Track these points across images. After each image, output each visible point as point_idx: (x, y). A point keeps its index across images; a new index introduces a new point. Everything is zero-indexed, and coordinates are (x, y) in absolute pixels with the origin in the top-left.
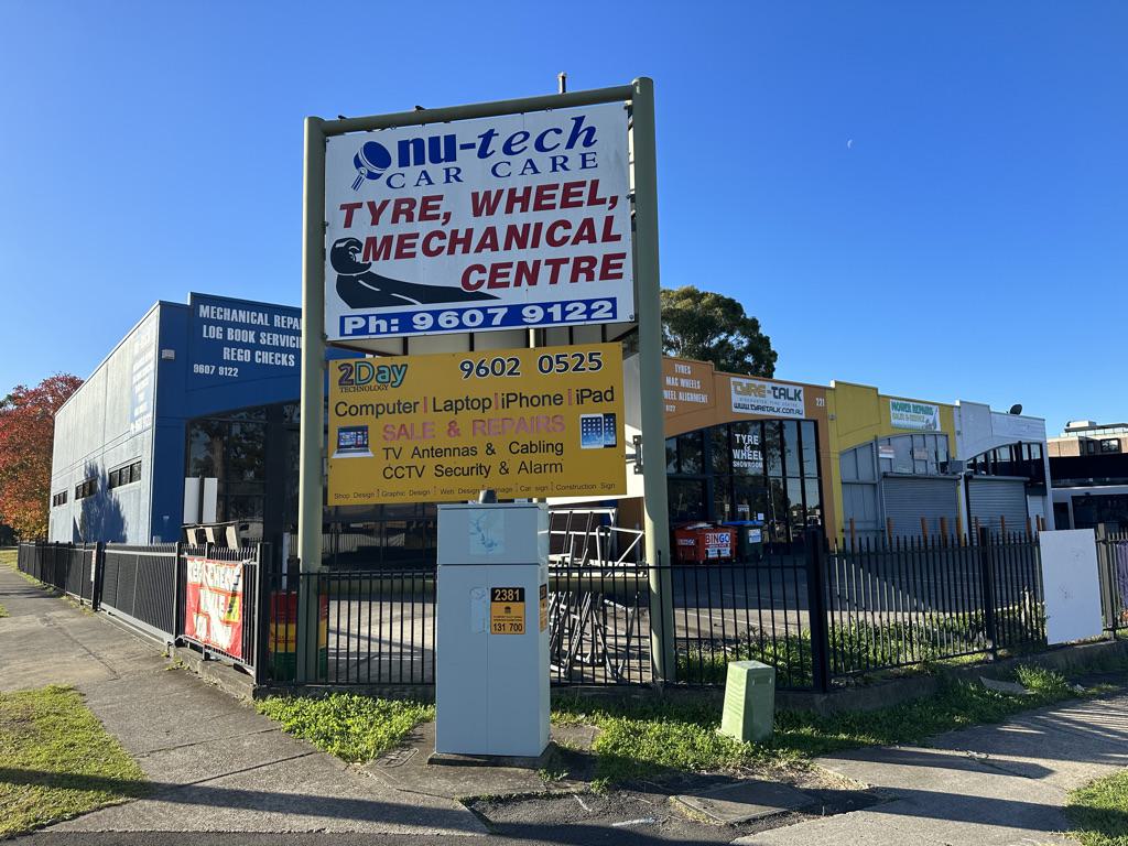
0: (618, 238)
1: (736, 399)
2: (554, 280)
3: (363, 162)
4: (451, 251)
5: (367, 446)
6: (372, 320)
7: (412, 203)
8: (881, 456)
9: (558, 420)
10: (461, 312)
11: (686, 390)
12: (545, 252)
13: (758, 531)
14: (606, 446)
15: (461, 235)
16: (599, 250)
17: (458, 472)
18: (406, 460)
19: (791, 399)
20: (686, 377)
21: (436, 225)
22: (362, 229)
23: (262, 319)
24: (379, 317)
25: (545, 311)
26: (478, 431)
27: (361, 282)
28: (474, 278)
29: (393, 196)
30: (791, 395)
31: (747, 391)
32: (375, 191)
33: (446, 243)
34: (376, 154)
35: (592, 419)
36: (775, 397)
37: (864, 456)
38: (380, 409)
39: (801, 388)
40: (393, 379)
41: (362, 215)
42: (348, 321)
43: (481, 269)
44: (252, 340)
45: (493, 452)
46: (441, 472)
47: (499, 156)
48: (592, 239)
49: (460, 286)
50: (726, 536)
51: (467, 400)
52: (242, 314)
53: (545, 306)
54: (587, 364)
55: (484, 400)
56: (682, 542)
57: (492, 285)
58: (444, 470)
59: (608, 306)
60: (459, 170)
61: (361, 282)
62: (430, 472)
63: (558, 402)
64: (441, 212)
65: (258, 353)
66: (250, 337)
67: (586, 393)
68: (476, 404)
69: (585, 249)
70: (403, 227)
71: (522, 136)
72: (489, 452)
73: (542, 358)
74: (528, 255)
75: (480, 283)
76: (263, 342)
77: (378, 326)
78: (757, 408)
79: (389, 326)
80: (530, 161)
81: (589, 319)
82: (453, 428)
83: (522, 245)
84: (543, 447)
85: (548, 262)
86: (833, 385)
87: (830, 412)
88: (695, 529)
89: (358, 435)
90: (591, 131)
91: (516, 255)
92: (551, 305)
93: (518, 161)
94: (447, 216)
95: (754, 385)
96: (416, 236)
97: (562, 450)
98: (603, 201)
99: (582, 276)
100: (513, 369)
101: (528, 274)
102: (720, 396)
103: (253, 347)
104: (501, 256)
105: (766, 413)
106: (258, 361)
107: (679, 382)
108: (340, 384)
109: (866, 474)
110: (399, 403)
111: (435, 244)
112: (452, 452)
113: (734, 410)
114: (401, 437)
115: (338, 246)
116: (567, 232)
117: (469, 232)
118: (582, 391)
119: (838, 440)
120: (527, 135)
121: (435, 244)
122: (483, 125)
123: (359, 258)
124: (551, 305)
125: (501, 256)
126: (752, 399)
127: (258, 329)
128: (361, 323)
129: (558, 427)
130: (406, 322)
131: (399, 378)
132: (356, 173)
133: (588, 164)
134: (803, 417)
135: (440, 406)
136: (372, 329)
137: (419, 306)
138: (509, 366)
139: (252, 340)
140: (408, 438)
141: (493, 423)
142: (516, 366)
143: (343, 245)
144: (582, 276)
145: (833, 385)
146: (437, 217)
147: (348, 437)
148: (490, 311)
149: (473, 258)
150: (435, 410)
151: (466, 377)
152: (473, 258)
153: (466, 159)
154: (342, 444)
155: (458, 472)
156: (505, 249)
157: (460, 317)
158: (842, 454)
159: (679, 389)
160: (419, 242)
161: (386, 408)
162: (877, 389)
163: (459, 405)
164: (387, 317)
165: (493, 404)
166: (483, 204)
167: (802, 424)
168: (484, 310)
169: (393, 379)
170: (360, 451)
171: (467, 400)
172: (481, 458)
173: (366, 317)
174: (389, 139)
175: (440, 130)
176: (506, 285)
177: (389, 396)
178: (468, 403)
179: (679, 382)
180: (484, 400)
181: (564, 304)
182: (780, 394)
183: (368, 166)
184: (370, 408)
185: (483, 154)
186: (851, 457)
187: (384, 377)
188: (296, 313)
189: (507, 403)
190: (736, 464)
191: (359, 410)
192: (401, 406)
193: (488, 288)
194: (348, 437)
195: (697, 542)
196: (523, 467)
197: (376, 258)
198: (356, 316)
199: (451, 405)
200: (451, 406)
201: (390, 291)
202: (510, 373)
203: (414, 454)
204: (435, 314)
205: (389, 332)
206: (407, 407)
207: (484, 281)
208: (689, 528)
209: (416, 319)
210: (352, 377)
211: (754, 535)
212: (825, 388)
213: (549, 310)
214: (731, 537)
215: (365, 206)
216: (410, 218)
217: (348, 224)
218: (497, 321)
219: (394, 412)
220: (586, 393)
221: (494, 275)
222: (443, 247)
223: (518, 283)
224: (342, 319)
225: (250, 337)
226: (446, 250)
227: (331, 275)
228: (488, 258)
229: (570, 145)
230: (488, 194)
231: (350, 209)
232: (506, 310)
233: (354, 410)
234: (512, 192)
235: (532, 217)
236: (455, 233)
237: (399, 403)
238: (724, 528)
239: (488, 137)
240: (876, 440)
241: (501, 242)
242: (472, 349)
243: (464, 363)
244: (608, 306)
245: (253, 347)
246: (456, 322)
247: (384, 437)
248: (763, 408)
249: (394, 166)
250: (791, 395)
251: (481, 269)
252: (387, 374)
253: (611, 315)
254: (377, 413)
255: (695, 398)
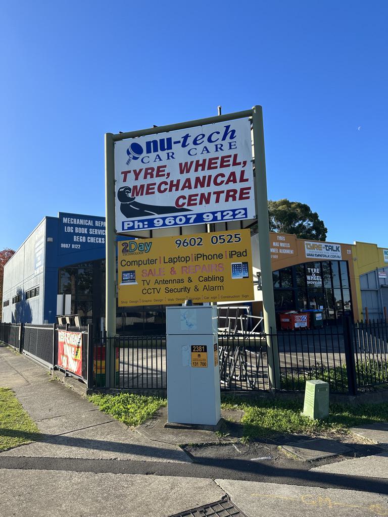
0: (247, 180)
1: (307, 251)
2: (217, 201)
3: (131, 152)
4: (171, 190)
5: (135, 279)
6: (136, 223)
7: (153, 169)
8: (379, 277)
9: (220, 265)
10: (175, 217)
11: (283, 248)
12: (213, 188)
13: (320, 314)
14: (244, 277)
15: (175, 183)
16: (238, 186)
17: (175, 290)
18: (152, 285)
19: (335, 251)
20: (283, 242)
21: (163, 179)
22: (131, 182)
23: (90, 223)
24: (139, 221)
25: (214, 215)
28: (181, 202)
29: (144, 167)
30: (335, 249)
31: (313, 248)
32: (136, 165)
33: (168, 187)
34: (137, 148)
35: (236, 265)
36: (327, 250)
37: (371, 278)
39: (339, 246)
40: (146, 249)
41: (131, 176)
42: (126, 224)
43: (184, 198)
45: (191, 281)
46: (169, 291)
47: (191, 146)
48: (235, 181)
50: (305, 317)
51: (179, 257)
53: (213, 213)
54: (233, 239)
55: (186, 257)
56: (283, 320)
57: (189, 204)
58: (169, 290)
59: (243, 212)
60: (173, 154)
62: (163, 291)
64: (166, 173)
66: (85, 231)
67: (234, 253)
68: (183, 259)
69: (231, 186)
70: (149, 180)
71: (201, 136)
72: (190, 281)
74: (205, 190)
75: (184, 204)
76: (91, 233)
77: (139, 225)
78: (318, 256)
79: (144, 225)
80: (205, 147)
81: (234, 218)
83: (202, 186)
84: (214, 278)
85: (215, 193)
86: (355, 243)
87: (354, 256)
88: (289, 314)
90: (233, 132)
91: (200, 190)
92: (216, 212)
93: (200, 148)
94: (168, 174)
95: (316, 245)
96: (155, 184)
98: (239, 164)
99: (231, 199)
101: (206, 199)
102: (300, 250)
103: (87, 235)
104: (193, 191)
105: (323, 258)
106: (89, 241)
107: (279, 244)
108: (123, 252)
109: (372, 286)
110: (148, 260)
111: (163, 187)
112: (173, 281)
113: (307, 257)
115: (121, 190)
116: (223, 179)
117: (178, 181)
119: (358, 270)
120: (204, 136)
121: (163, 187)
122: (183, 132)
123: (130, 195)
124: (216, 212)
125: (193, 191)
126: (315, 252)
127: (89, 227)
128: (131, 224)
129: (221, 269)
130: (151, 223)
131: (148, 248)
133: (232, 147)
134: (341, 259)
136: (136, 227)
137: (156, 216)
138: (198, 241)
140: (153, 275)
143: (123, 190)
144: (231, 199)
145: (355, 243)
147: (126, 275)
148: (188, 217)
149: (180, 193)
150: (164, 263)
151: (178, 247)
152: (180, 193)
153: (176, 148)
155: (175, 290)
157: (175, 220)
158: (361, 276)
159: (279, 248)
160: (156, 187)
162: (376, 245)
164: (143, 221)
166: (184, 168)
167: (340, 262)
168: (185, 216)
169: (146, 249)
170: (132, 282)
171: (179, 257)
172: (186, 284)
173: (133, 222)
174: (142, 141)
175: (164, 136)
176: (196, 204)
177: (144, 257)
178: (179, 259)
179: (279, 244)
180: (186, 257)
181: (222, 212)
182: (329, 249)
183: (133, 154)
185: (184, 145)
186: (365, 279)
187: (142, 248)
188: (103, 219)
189: (197, 258)
190: (308, 283)
191: (131, 263)
194: (126, 275)
195: (290, 320)
197: (137, 195)
199: (172, 260)
200: (172, 260)
201: (144, 209)
204: (164, 219)
205: (144, 228)
206: (153, 262)
208: (287, 313)
209: (155, 221)
210: (128, 249)
211: (319, 317)
212: (351, 245)
213: (216, 215)
214: (307, 318)
215: (132, 172)
216: (152, 177)
217: (125, 180)
218: (192, 221)
219: (146, 264)
220: (234, 253)
221: (190, 200)
223: (201, 203)
224: (123, 223)
225: (85, 231)
227: (118, 203)
228: (187, 192)
229: (224, 139)
230: (186, 164)
231: (126, 173)
232: (195, 216)
234: (198, 162)
238: (303, 313)
239: (186, 137)
240: (377, 269)
242: (181, 234)
244: (243, 212)
245: (87, 235)
246: (173, 222)
247: (142, 275)
248: (321, 256)
249: (145, 153)
250: (335, 249)
251: (184, 198)
252: (143, 247)
253: (244, 216)
255: (288, 251)
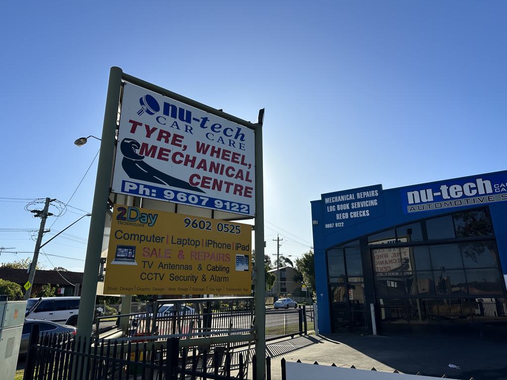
0: (251, 181)
2: (227, 191)
3: (144, 103)
4: (186, 164)
5: (134, 258)
6: (141, 187)
7: (169, 135)
9: (228, 256)
10: (188, 195)
12: (224, 178)
14: (245, 270)
15: (191, 158)
16: (245, 184)
17: (182, 278)
18: (155, 269)
21: (180, 150)
22: (140, 136)
23: (352, 197)
24: (145, 186)
25: (224, 204)
26: (221, 259)
27: (137, 164)
28: (195, 180)
29: (160, 127)
32: (148, 120)
33: (184, 159)
34: (153, 104)
35: (240, 257)
38: (143, 238)
40: (149, 221)
41: (141, 131)
42: (127, 184)
43: (199, 177)
44: (348, 208)
45: (201, 269)
46: (173, 278)
47: (209, 130)
48: (242, 178)
49: (189, 182)
51: (189, 240)
52: (342, 197)
53: (224, 202)
54: (235, 230)
55: (196, 241)
57: (203, 186)
58: (174, 277)
59: (247, 208)
60: (192, 129)
61: (137, 164)
62: (167, 277)
63: (229, 248)
64: (183, 144)
65: (351, 213)
66: (347, 206)
67: (210, 242)
68: (193, 243)
69: (238, 181)
70: (162, 144)
71: (219, 126)
72: (200, 269)
73: (219, 224)
74: (219, 177)
75: (197, 183)
76: (353, 207)
77: (144, 191)
79: (151, 193)
80: (221, 137)
81: (240, 212)
82: (181, 254)
83: (216, 172)
84: (221, 269)
85: (225, 183)
89: (129, 251)
90: (243, 135)
91: (213, 175)
92: (226, 202)
93: (217, 136)
94: (185, 147)
96: (169, 151)
97: (229, 271)
98: (246, 165)
99: (238, 193)
100: (209, 227)
101: (217, 185)
103: (348, 211)
104: (207, 174)
106: (352, 217)
108: (117, 219)
110: (154, 236)
111: (178, 158)
112: (180, 267)
114: (153, 255)
115: (125, 141)
116: (233, 172)
117: (195, 158)
118: (209, 241)
120: (220, 127)
121: (178, 158)
122: (205, 114)
123: (138, 152)
124: (226, 202)
125: (207, 174)
127: (350, 202)
128: (135, 187)
129: (227, 259)
130: (160, 193)
131: (153, 221)
132: (140, 107)
133: (242, 148)
135: (175, 241)
136: (141, 192)
137: (167, 186)
138: (207, 225)
139: (348, 208)
140: (157, 257)
141: (200, 254)
142: (210, 226)
143: (129, 142)
144: (238, 193)
146: (180, 146)
147: (123, 251)
148: (201, 198)
149: (195, 171)
150: (172, 243)
151: (186, 226)
152: (195, 171)
153: (195, 125)
154: (118, 255)
155: (182, 278)
156: (197, 168)
157: (187, 197)
160: (171, 154)
161: (146, 238)
163: (185, 242)
164: (151, 188)
165: (201, 243)
166: (201, 148)
168: (199, 196)
169: (149, 221)
170: (130, 261)
171: (189, 240)
172: (195, 272)
173: (138, 185)
174: (161, 100)
175: (187, 107)
176: (209, 187)
177: (146, 230)
178: (189, 242)
180: (196, 241)
181: (231, 203)
183: (146, 106)
184: (137, 236)
185: (202, 126)
187: (144, 220)
188: (252, 189)
189: (208, 244)
191: (130, 237)
192: (155, 238)
193: (201, 187)
194: (123, 251)
196: (212, 278)
197: (147, 154)
198: (132, 183)
199: (181, 241)
200: (181, 242)
201: (152, 174)
202: (207, 229)
203: (160, 266)
204: (176, 193)
205: (150, 196)
206: (159, 239)
207: (199, 183)
209: (166, 192)
210: (125, 216)
213: (225, 204)
215: (144, 125)
216: (167, 141)
217: (133, 131)
218: (204, 203)
219: (150, 241)
220: (239, 246)
221: (204, 182)
222: (182, 161)
223: (213, 188)
224: (124, 182)
225: (347, 206)
226: (183, 162)
227: (120, 156)
228: (201, 173)
229: (236, 138)
230: (203, 144)
231: (135, 124)
232: (207, 199)
233: (126, 236)
234: (213, 147)
235: (221, 161)
236: (188, 156)
237: (154, 236)
239: (205, 120)
241: (196, 164)
242: (176, 212)
243: (187, 219)
244: (247, 208)
245: (348, 211)
246: (185, 199)
247: (144, 255)
249: (161, 113)
251: (199, 177)
252: (146, 218)
253: (247, 212)
254: (141, 240)
